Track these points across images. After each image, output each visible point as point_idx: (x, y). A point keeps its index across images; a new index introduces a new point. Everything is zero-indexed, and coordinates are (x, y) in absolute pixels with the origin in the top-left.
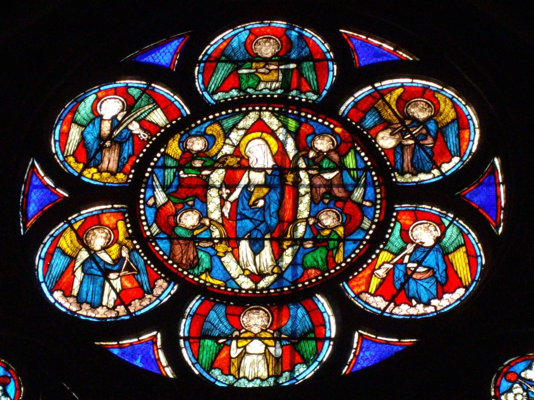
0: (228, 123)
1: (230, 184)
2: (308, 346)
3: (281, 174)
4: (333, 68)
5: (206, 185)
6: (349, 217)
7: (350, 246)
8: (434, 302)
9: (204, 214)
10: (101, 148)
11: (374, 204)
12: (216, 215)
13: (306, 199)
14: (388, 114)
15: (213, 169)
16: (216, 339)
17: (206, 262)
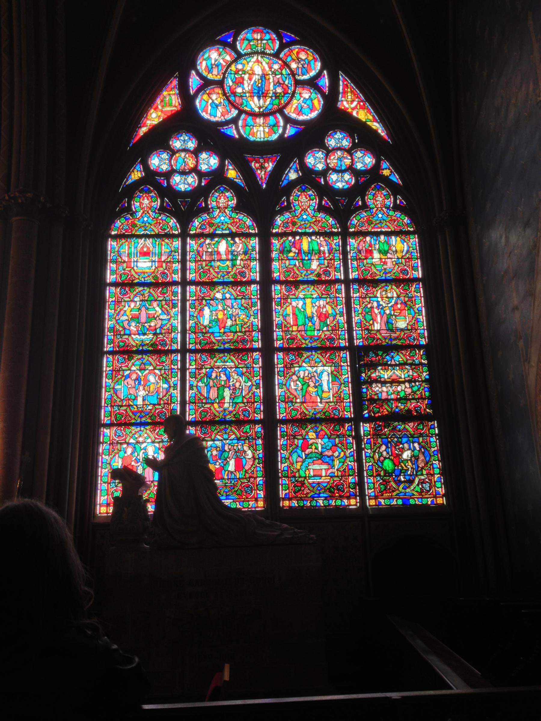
0: (248, 60)
1: (250, 79)
2: (275, 128)
3: (264, 76)
4: (278, 42)
5: (243, 79)
6: (285, 89)
7: (285, 98)
8: (309, 115)
9: (243, 89)
10: (212, 68)
11: (291, 85)
12: (247, 89)
13: (272, 84)
14: (294, 57)
15: (245, 74)
16: (250, 126)
17: (245, 104)
